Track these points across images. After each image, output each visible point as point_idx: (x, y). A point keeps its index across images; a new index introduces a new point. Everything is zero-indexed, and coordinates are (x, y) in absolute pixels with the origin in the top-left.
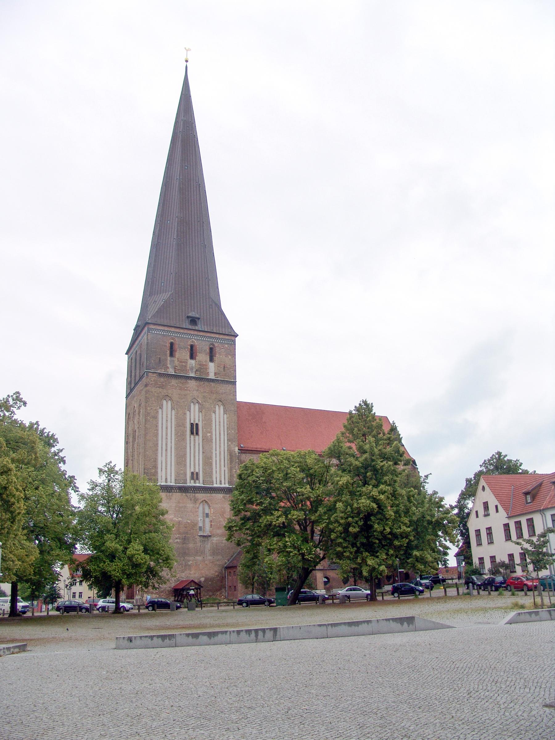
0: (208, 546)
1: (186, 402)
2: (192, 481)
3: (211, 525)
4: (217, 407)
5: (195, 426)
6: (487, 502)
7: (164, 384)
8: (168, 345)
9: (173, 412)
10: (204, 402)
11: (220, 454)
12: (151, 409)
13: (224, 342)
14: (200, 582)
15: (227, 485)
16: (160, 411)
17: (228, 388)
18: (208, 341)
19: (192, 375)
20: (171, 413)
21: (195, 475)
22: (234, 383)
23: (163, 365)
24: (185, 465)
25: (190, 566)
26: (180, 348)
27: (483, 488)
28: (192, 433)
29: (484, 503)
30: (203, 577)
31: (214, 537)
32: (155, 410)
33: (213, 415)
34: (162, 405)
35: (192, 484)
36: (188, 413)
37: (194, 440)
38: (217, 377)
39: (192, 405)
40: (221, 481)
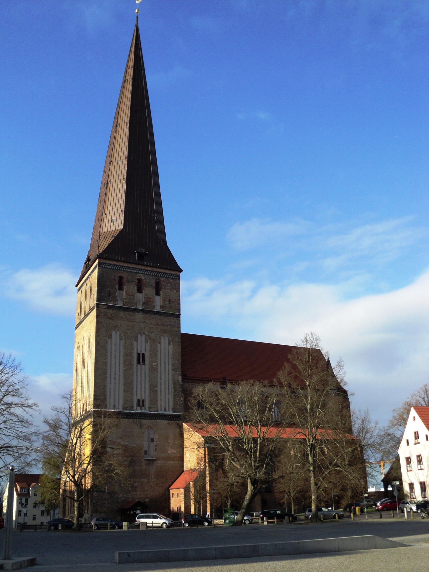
1: (134, 334)
2: (139, 408)
3: (156, 449)
4: (162, 338)
5: (141, 356)
7: (113, 315)
8: (117, 279)
10: (151, 333)
11: (165, 383)
12: (101, 339)
13: (169, 277)
14: (145, 502)
15: (171, 413)
16: (109, 341)
17: (173, 321)
18: (154, 275)
19: (140, 307)
20: (120, 343)
21: (141, 403)
22: (179, 316)
24: (132, 393)
26: (129, 282)
28: (139, 362)
29: (415, 433)
30: (148, 498)
31: (158, 460)
32: (105, 340)
33: (159, 345)
34: (111, 335)
36: (135, 343)
38: (163, 310)
39: (139, 335)
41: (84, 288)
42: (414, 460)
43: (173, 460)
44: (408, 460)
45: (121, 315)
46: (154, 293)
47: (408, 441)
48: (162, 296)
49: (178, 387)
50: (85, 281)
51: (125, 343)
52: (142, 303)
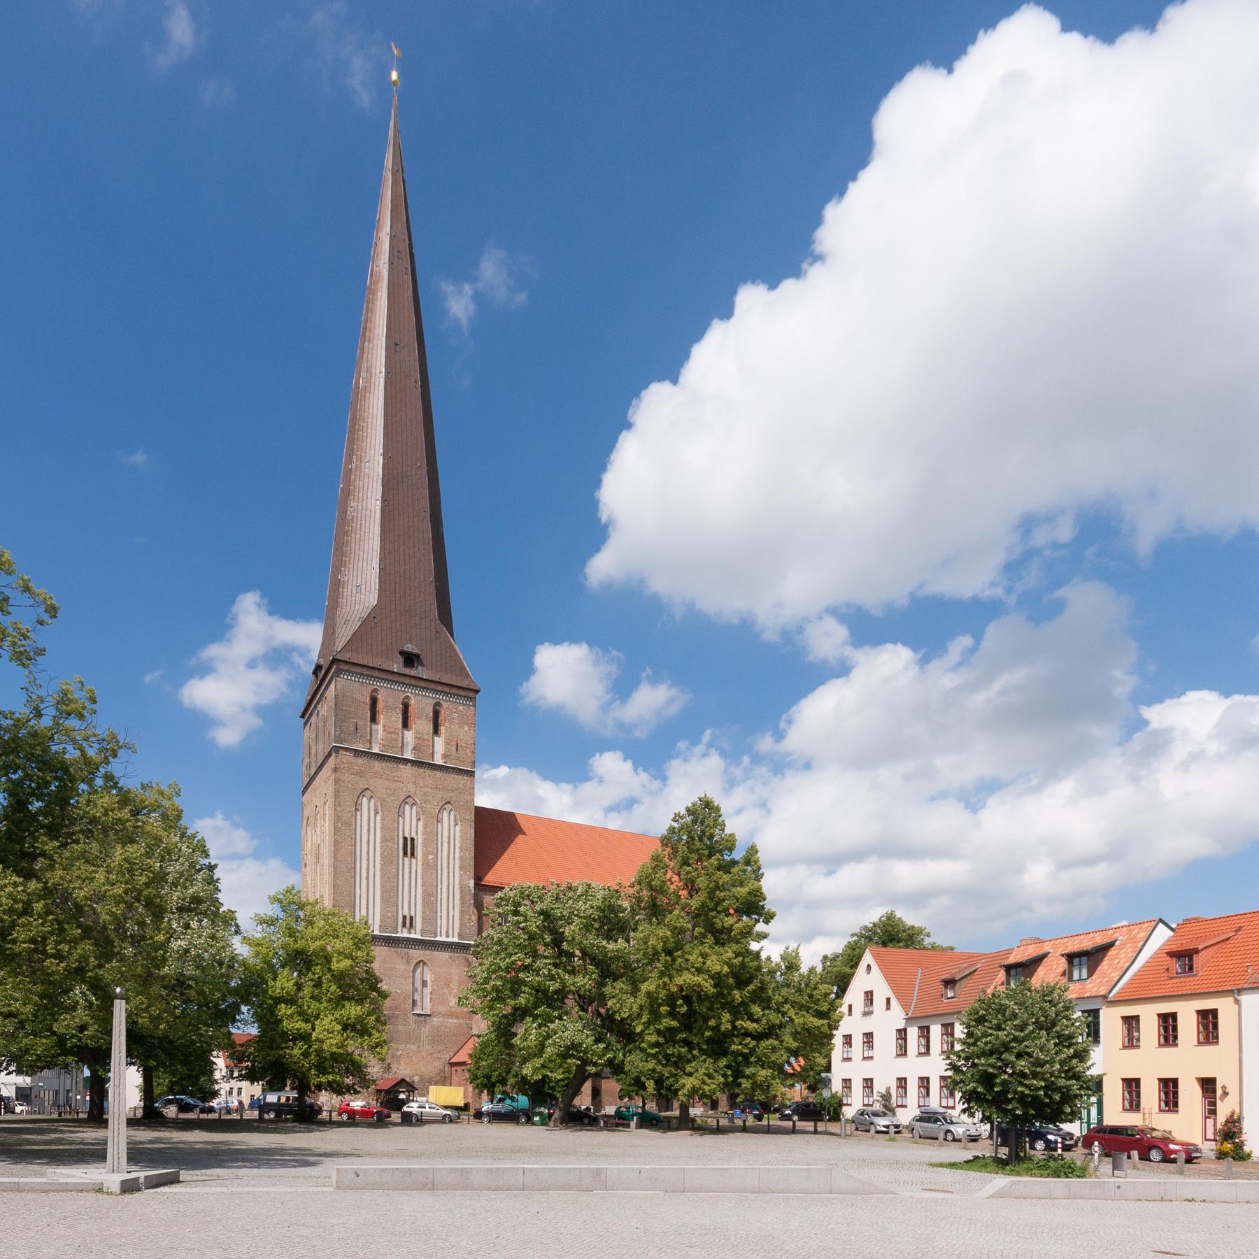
0: (426, 1031)
6: (871, 992)
9: (379, 817)
14: (413, 1082)
15: (456, 940)
18: (432, 697)
21: (408, 922)
23: (362, 736)
25: (399, 1057)
26: (388, 708)
27: (869, 967)
28: (405, 854)
29: (866, 993)
30: (417, 1075)
35: (406, 935)
37: (410, 865)
38: (445, 762)
40: (447, 932)
41: (313, 719)
42: (858, 1041)
43: (457, 1017)
44: (848, 1040)
45: (376, 768)
46: (431, 731)
47: (850, 1006)
48: (443, 735)
49: (468, 897)
50: (315, 707)
51: (383, 819)
52: (411, 748)
